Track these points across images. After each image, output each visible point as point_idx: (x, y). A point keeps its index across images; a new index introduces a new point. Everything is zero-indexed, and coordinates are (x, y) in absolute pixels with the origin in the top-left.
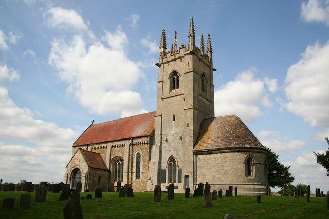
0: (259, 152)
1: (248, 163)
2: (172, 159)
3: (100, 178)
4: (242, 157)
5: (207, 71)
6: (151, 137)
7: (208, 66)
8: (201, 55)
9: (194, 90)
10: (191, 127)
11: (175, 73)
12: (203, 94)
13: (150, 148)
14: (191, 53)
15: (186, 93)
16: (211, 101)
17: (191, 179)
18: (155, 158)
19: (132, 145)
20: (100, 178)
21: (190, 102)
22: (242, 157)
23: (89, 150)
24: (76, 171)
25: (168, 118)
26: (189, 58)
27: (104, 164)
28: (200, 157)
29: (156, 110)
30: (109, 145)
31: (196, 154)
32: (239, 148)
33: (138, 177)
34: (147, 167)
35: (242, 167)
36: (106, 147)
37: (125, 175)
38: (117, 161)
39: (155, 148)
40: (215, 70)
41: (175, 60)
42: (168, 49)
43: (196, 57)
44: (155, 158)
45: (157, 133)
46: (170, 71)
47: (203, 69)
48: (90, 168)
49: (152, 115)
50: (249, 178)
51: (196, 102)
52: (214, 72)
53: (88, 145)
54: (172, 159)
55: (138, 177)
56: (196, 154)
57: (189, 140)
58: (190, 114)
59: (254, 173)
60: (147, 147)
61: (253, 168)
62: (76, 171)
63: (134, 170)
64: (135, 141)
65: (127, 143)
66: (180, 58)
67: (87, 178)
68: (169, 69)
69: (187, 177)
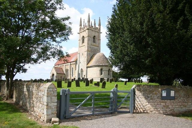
0: (106, 67)
1: (101, 70)
2: (82, 69)
3: (61, 77)
4: (99, 69)
5: (96, 34)
6: (76, 61)
7: (98, 32)
8: (94, 29)
9: (88, 44)
10: (86, 58)
11: (83, 37)
12: (95, 44)
13: (76, 65)
14: (88, 29)
15: (86, 45)
17: (85, 76)
18: (77, 69)
20: (61, 77)
21: (87, 49)
22: (99, 69)
23: (59, 67)
24: (53, 75)
25: (81, 54)
27: (63, 72)
28: (88, 69)
29: (78, 51)
30: (64, 65)
31: (87, 67)
32: (98, 65)
33: (72, 76)
34: (75, 72)
35: (99, 72)
36: (63, 66)
37: (69, 75)
38: (67, 70)
39: (77, 66)
40: (101, 33)
41: (83, 31)
42: (82, 27)
43: (90, 30)
44: (77, 69)
45: (78, 60)
46: (82, 36)
47: (94, 34)
48: (57, 73)
49: (76, 54)
50: (101, 76)
51: (89, 48)
52: (101, 34)
53: (59, 65)
54: (82, 69)
55: (72, 76)
56: (87, 67)
57: (86, 63)
58: (86, 53)
59: (103, 74)
60: (75, 65)
61: (103, 72)
62: (53, 75)
63: (71, 74)
64: (72, 63)
65: (69, 64)
66: (85, 31)
67: (56, 77)
68: (82, 35)
69: (85, 75)
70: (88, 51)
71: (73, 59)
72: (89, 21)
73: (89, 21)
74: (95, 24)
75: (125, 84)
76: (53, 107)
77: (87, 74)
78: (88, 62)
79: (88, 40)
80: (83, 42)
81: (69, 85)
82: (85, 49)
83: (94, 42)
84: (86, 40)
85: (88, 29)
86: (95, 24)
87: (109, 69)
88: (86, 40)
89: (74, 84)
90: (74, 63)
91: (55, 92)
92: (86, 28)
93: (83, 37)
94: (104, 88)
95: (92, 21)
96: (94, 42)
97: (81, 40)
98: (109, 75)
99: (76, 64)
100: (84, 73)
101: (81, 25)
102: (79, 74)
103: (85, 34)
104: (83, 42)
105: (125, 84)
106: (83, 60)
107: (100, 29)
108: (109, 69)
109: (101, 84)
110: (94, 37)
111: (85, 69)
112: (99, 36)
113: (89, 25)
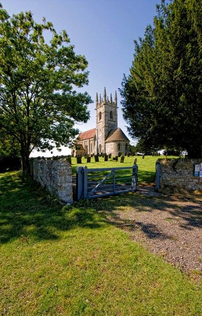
1: (119, 145)
5: (113, 110)
6: (95, 137)
9: (105, 120)
11: (100, 113)
14: (105, 104)
16: (116, 122)
18: (96, 145)
19: (89, 141)
26: (104, 106)
30: (84, 141)
31: (105, 143)
38: (86, 147)
39: (96, 142)
42: (99, 102)
44: (96, 145)
47: (110, 109)
56: (105, 143)
57: (104, 138)
64: (91, 139)
67: (77, 153)
70: (105, 126)
71: (93, 135)
72: (105, 96)
73: (105, 96)
74: (111, 100)
75: (143, 158)
76: (68, 188)
77: (105, 149)
78: (107, 137)
79: (106, 116)
80: (100, 118)
81: (89, 161)
82: (102, 125)
83: (111, 117)
84: (103, 116)
85: (105, 104)
86: (111, 100)
87: (127, 144)
88: (103, 116)
89: (93, 159)
90: (93, 139)
91: (69, 170)
92: (102, 104)
93: (100, 113)
94: (123, 162)
95: (108, 95)
96: (111, 117)
97: (99, 116)
98: (126, 149)
99: (95, 140)
100: (103, 148)
101: (97, 101)
102: (98, 149)
103: (102, 110)
104: (100, 118)
105: (143, 158)
106: (101, 135)
107: (116, 103)
108: (127, 144)
109: (119, 159)
110: (111, 112)
111: (103, 145)
112: (116, 112)
113: (106, 100)
